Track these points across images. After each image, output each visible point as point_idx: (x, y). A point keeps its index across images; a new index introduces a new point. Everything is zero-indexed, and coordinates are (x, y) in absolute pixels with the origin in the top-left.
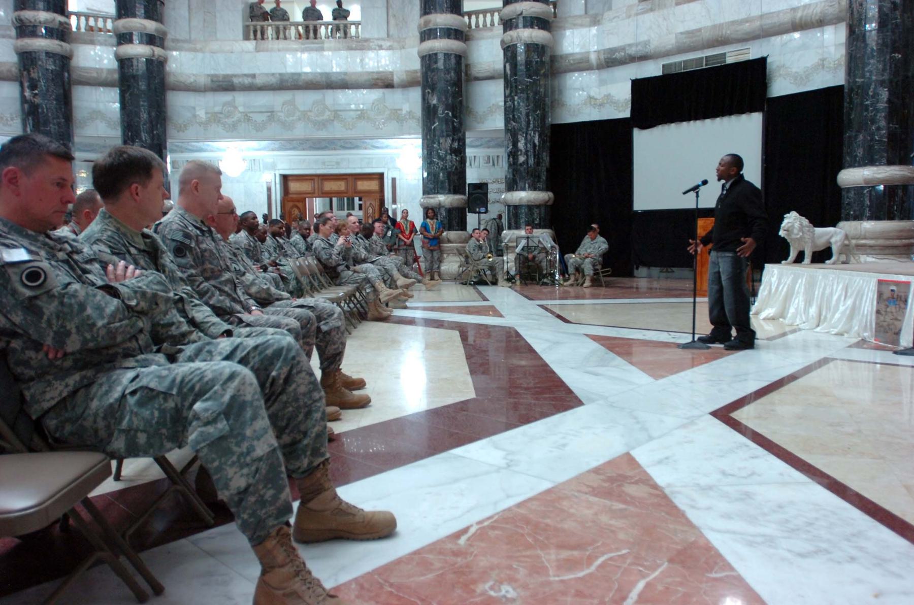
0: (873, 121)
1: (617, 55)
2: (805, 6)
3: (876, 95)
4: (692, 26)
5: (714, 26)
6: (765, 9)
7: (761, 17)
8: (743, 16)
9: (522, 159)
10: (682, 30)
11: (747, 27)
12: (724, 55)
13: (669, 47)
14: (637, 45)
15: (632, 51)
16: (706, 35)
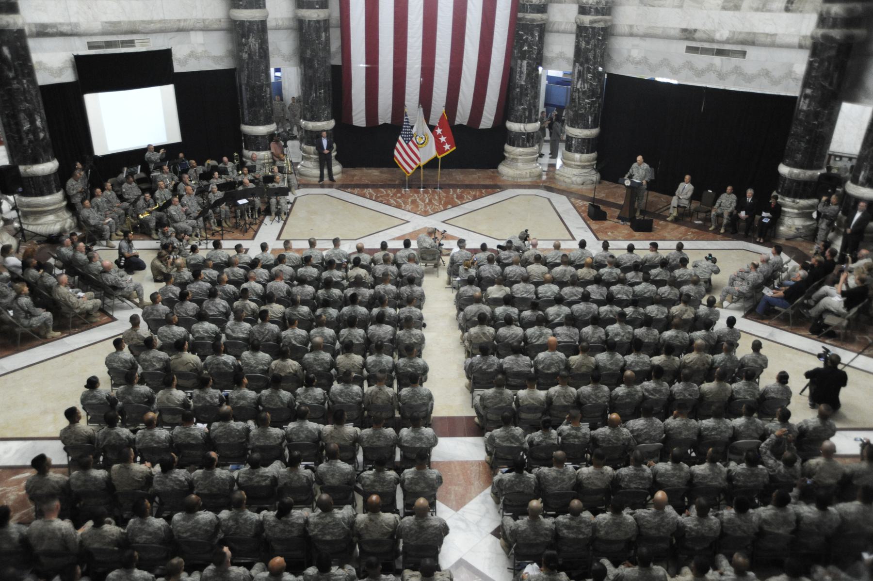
0: (266, 104)
1: (49, 30)
2: (185, 20)
3: (266, 91)
4: (114, 19)
5: (130, 22)
6: (160, 17)
7: (160, 21)
8: (147, 18)
9: (42, 135)
10: (105, 18)
11: (152, 27)
12: (131, 43)
13: (97, 31)
14: (70, 24)
15: (65, 29)
16: (125, 27)
